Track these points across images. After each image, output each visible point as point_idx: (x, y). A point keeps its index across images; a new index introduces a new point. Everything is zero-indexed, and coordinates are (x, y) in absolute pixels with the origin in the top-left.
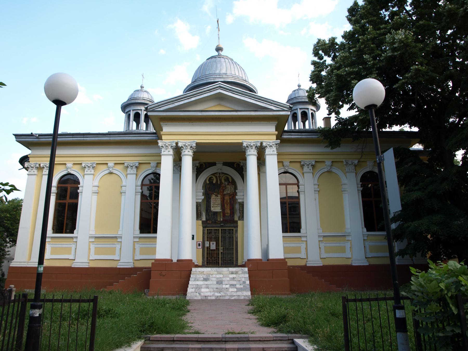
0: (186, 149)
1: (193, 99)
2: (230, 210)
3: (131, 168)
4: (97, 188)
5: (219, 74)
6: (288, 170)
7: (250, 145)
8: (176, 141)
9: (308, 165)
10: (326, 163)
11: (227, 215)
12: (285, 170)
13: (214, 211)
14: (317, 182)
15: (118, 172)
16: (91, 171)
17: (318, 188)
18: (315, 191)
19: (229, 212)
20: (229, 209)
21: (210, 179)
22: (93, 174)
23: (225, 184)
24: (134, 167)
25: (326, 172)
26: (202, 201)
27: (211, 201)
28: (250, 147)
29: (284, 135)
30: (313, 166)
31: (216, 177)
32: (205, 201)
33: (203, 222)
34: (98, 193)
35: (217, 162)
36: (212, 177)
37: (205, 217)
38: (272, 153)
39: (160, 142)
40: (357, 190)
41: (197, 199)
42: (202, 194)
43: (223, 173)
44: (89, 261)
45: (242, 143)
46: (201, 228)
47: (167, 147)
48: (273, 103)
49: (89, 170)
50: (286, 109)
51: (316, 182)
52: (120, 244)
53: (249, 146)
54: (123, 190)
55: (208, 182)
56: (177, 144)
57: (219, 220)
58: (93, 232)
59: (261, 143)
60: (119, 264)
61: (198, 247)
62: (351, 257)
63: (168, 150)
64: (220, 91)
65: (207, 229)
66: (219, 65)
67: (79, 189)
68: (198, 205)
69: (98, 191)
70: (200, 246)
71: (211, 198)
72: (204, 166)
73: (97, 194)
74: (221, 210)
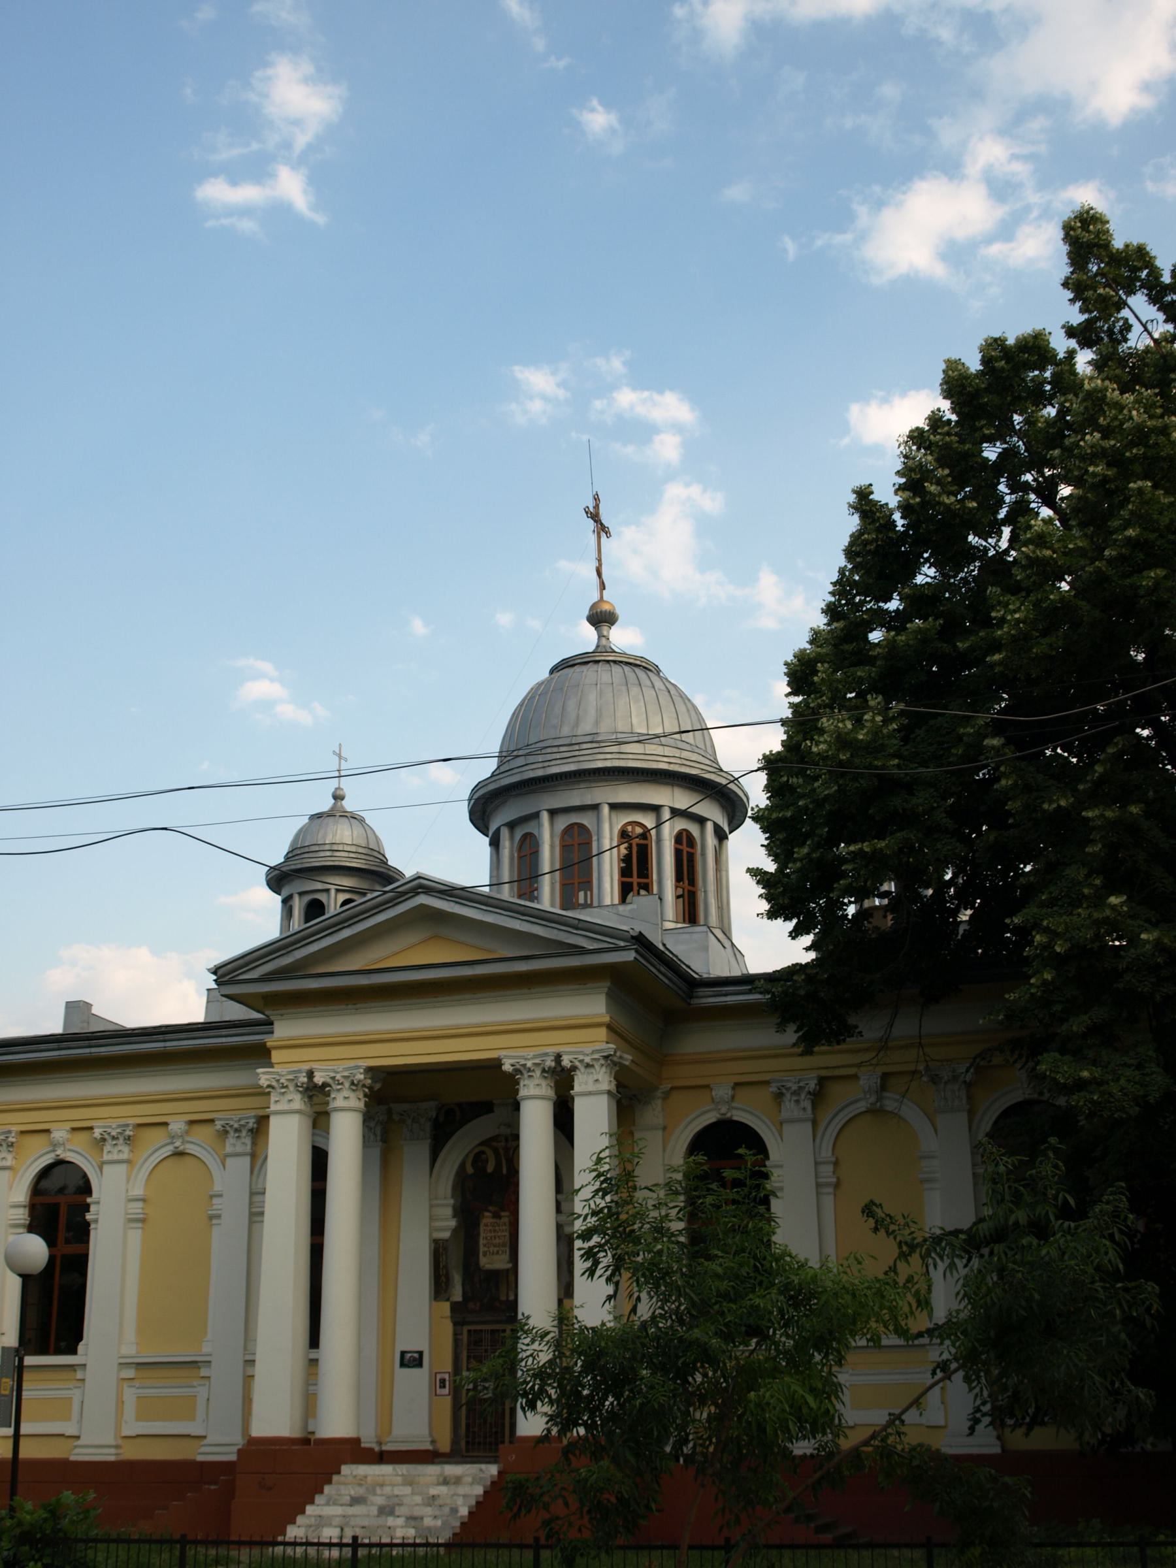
0: (339, 1090)
1: (346, 933)
3: (237, 1135)
4: (140, 1204)
5: (567, 741)
6: (729, 1115)
7: (524, 1065)
8: (306, 1067)
9: (794, 1093)
10: (861, 1082)
12: (718, 1116)
13: (488, 1267)
14: (830, 1153)
15: (199, 1149)
16: (120, 1151)
17: (834, 1173)
18: (818, 1185)
21: (478, 1159)
22: (128, 1162)
24: (244, 1133)
25: (865, 1112)
26: (451, 1236)
27: (479, 1234)
28: (525, 1072)
29: (698, 997)
30: (818, 1097)
31: (496, 1151)
33: (455, 1307)
34: (143, 1221)
35: (494, 1101)
36: (483, 1152)
37: (461, 1289)
38: (591, 1087)
39: (264, 1073)
40: (971, 1176)
41: (432, 1230)
42: (449, 1211)
44: (120, 1442)
45: (496, 1064)
46: (448, 1327)
47: (283, 1087)
48: (580, 926)
49: (115, 1150)
50: (622, 944)
51: (826, 1153)
52: (208, 1383)
53: (522, 1069)
54: (215, 1207)
55: (470, 1170)
56: (310, 1074)
57: (503, 1298)
58: (129, 1350)
59: (558, 1058)
60: (203, 1449)
61: (439, 1391)
62: (942, 1423)
63: (289, 1097)
64: (423, 899)
65: (469, 1331)
66: (571, 705)
67: (89, 1211)
68: (439, 1251)
69: (141, 1216)
70: (444, 1387)
71: (479, 1225)
73: (140, 1225)
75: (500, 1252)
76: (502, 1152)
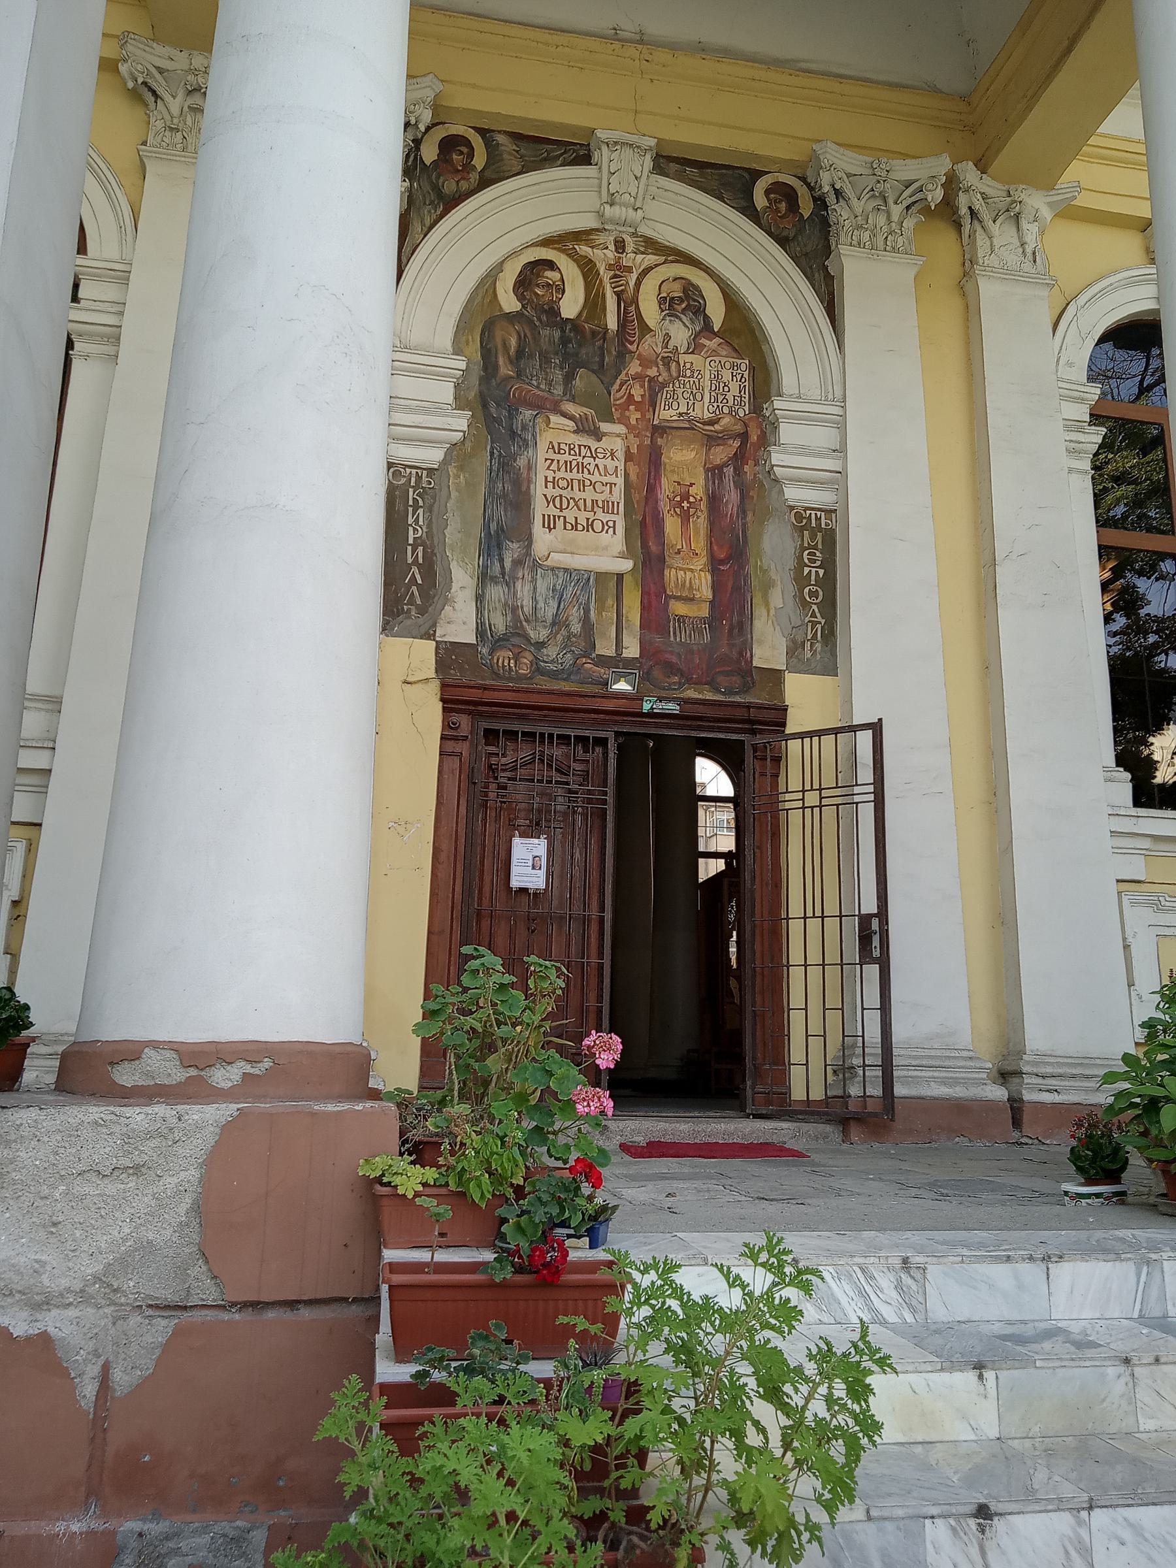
2: (714, 564)
11: (679, 608)
13: (556, 559)
19: (704, 586)
20: (700, 563)
23: (668, 336)
31: (588, 268)
32: (482, 464)
35: (600, 133)
36: (550, 265)
42: (445, 392)
43: (651, 245)
55: (509, 303)
72: (479, 161)
74: (626, 565)
75: (598, 526)
76: (606, 276)
